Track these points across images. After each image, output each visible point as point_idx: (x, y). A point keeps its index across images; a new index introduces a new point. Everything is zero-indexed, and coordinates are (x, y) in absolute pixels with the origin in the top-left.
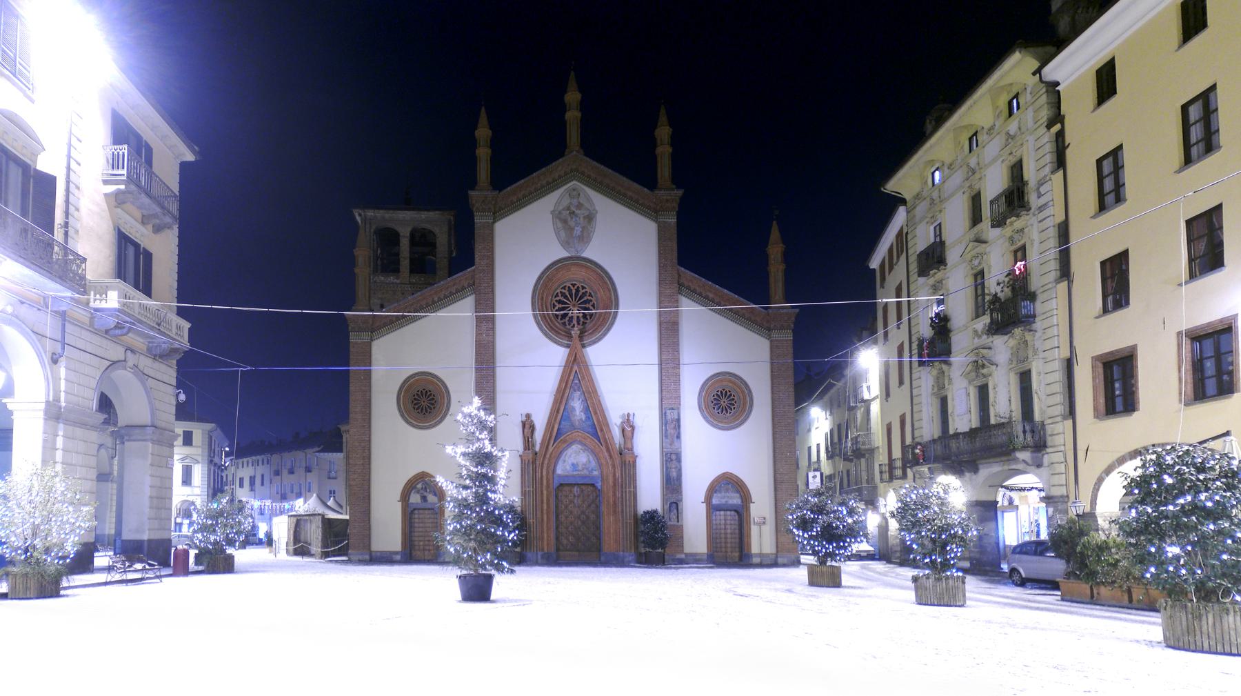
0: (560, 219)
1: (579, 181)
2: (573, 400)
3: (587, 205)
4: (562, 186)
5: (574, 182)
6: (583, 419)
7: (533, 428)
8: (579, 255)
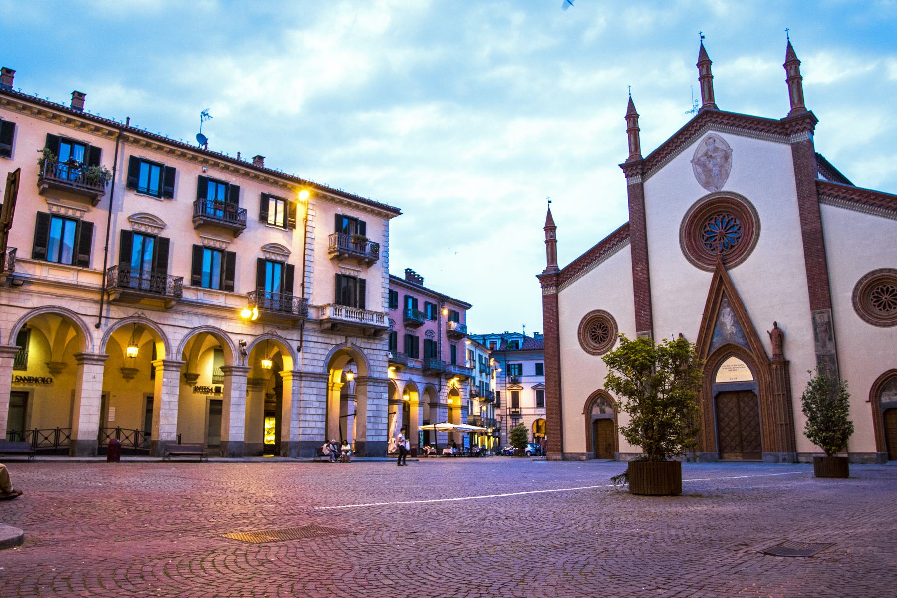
0: (699, 165)
2: (723, 317)
3: (722, 147)
5: (710, 131)
8: (718, 191)
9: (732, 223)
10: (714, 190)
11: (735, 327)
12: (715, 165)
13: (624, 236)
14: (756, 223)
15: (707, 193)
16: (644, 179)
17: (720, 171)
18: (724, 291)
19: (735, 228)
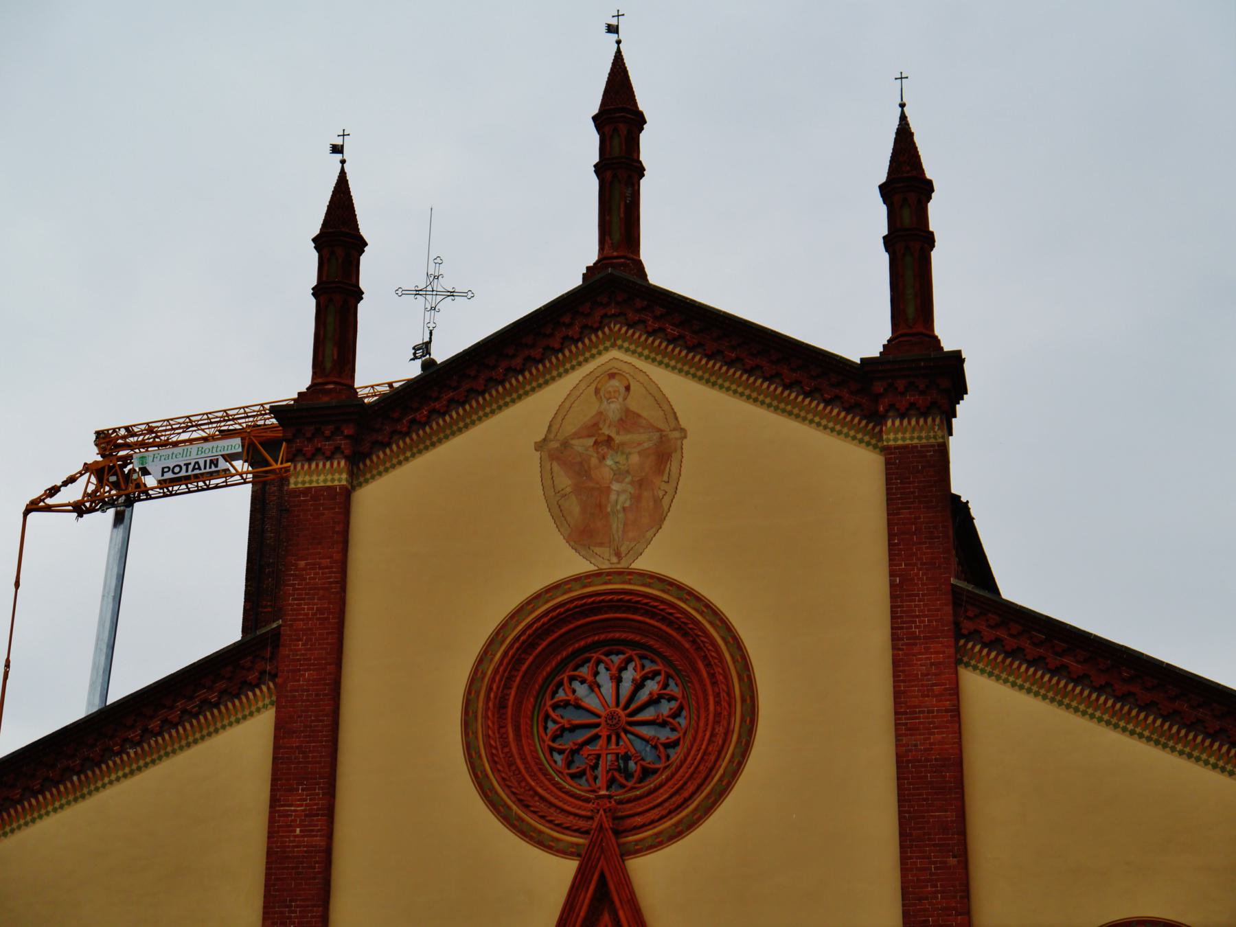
3: (650, 414)
4: (573, 368)
5: (615, 353)
8: (624, 564)
9: (652, 686)
10: (604, 561)
12: (619, 475)
13: (252, 677)
14: (743, 700)
15: (582, 566)
16: (358, 475)
17: (637, 499)
19: (665, 708)
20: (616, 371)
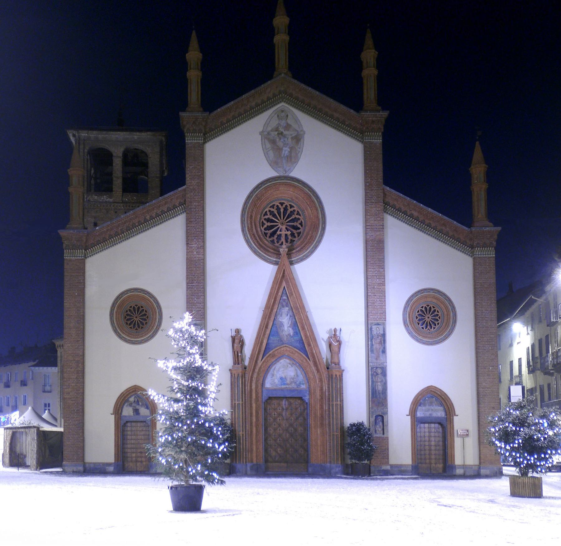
0: (268, 139)
1: (287, 103)
3: (295, 126)
4: (270, 108)
5: (283, 104)
6: (292, 334)
7: (242, 343)
8: (286, 174)
11: (293, 329)
18: (284, 287)
20: (283, 109)
